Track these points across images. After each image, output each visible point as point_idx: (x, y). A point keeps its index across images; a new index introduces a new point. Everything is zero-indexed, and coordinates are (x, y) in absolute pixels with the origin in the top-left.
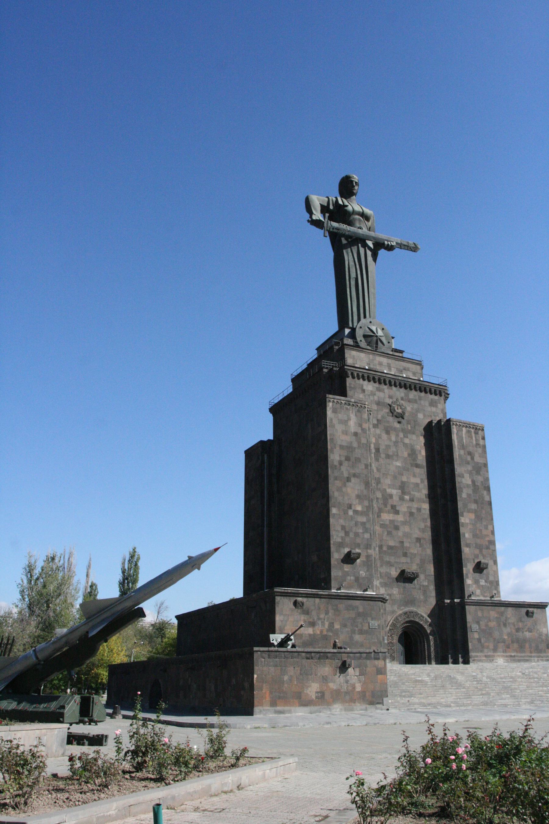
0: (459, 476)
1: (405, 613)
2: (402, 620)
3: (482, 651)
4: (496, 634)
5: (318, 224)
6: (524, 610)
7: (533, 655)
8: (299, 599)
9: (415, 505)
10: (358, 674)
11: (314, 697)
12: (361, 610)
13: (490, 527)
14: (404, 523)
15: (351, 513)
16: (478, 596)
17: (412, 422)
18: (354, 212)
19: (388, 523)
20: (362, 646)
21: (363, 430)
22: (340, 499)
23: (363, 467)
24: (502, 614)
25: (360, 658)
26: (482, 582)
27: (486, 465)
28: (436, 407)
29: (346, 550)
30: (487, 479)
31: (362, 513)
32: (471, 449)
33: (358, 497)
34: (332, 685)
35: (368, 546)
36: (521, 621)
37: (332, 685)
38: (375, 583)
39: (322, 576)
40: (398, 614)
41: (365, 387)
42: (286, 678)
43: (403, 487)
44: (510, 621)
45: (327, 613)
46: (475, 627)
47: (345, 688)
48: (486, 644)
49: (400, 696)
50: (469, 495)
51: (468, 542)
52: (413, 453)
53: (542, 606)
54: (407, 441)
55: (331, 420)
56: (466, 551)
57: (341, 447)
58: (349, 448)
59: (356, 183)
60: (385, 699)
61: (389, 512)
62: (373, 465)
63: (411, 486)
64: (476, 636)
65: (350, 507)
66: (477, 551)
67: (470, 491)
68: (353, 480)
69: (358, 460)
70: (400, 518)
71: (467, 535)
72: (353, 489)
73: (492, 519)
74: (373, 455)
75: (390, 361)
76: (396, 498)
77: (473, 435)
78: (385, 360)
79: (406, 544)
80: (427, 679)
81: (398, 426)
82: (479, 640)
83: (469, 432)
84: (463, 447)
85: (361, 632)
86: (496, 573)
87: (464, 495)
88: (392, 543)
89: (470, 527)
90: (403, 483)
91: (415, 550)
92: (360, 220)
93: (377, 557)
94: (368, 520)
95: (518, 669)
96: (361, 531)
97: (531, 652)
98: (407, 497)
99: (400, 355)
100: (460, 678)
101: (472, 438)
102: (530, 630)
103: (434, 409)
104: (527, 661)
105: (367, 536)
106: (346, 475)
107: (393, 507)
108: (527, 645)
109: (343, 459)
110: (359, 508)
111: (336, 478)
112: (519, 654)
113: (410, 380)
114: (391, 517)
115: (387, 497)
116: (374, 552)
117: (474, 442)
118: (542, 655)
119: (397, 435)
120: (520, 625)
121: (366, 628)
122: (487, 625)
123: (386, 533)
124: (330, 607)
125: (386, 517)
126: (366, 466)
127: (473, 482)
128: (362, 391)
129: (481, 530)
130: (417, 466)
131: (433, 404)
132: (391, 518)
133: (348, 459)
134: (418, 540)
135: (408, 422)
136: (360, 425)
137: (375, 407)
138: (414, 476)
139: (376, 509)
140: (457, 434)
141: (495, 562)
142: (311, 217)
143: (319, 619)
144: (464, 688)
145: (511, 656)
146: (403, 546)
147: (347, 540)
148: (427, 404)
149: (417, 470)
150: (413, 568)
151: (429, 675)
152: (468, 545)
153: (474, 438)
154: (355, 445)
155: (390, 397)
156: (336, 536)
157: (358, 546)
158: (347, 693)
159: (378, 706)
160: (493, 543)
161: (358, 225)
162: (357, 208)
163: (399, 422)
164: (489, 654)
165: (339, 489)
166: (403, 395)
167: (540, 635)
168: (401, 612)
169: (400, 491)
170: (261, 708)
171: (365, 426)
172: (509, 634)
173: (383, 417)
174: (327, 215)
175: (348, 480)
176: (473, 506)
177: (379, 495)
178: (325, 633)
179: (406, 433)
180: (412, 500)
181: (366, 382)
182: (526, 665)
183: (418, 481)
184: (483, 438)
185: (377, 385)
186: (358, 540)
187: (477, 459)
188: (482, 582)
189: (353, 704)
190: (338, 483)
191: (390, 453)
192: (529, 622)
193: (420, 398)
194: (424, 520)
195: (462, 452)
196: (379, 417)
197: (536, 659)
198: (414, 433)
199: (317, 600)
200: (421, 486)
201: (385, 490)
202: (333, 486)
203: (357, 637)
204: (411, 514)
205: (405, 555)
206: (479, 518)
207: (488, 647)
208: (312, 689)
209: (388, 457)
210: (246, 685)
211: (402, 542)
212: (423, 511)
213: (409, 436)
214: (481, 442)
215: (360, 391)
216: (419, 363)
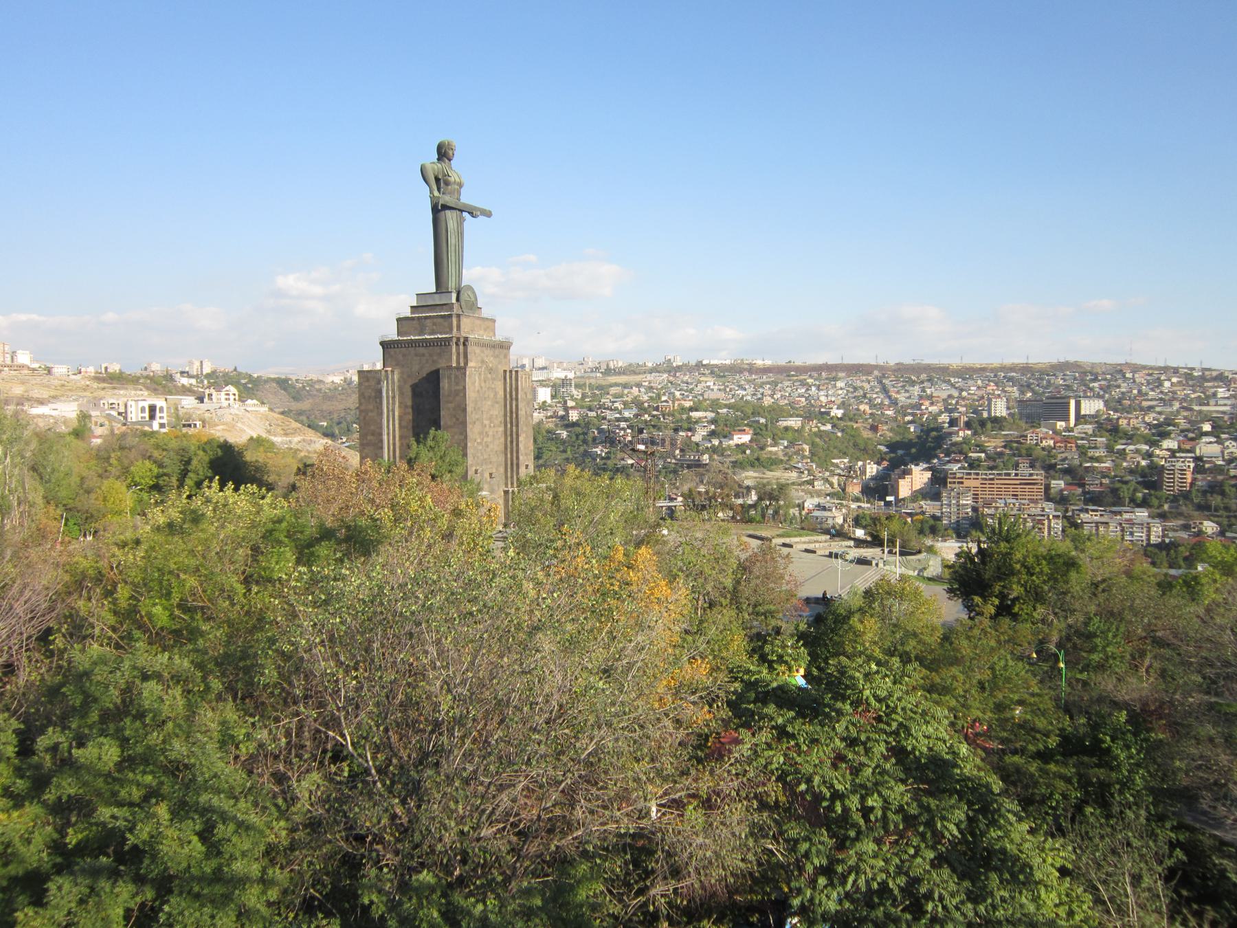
43: (490, 419)
52: (496, 394)
91: (494, 459)
179: (493, 379)
202: (469, 427)
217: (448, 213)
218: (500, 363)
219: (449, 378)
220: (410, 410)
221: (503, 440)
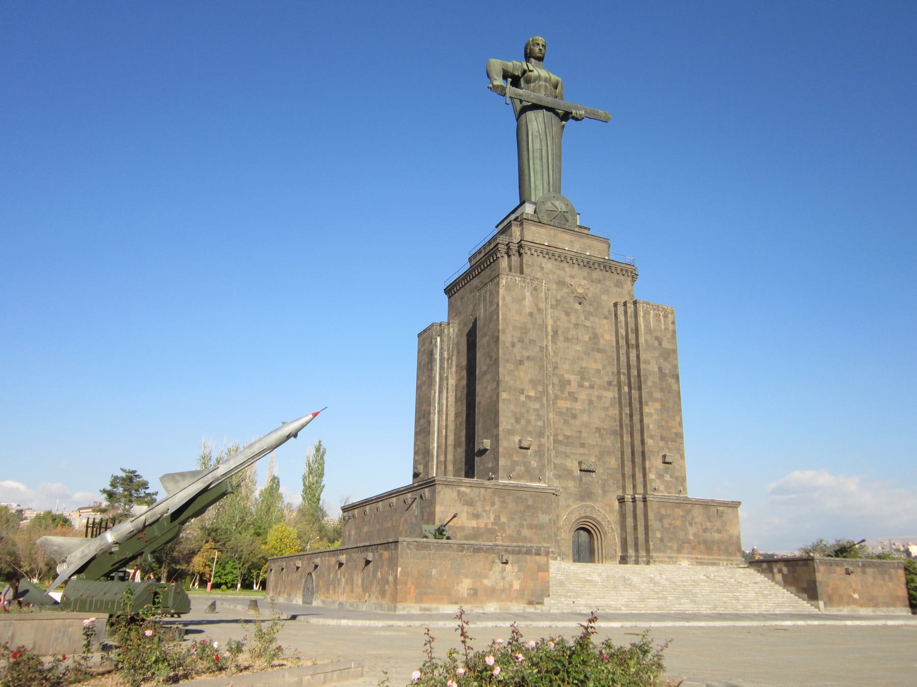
1: (582, 507)
2: (576, 516)
3: (664, 552)
4: (681, 534)
5: (501, 91)
7: (722, 557)
8: (463, 489)
9: (596, 392)
10: (516, 570)
11: (465, 595)
12: (530, 503)
13: (678, 419)
14: (583, 411)
15: (523, 398)
17: (595, 304)
18: (539, 78)
19: (564, 410)
20: (531, 541)
21: (539, 309)
22: (511, 383)
23: (538, 349)
24: (689, 511)
25: (519, 552)
26: (667, 477)
28: (622, 288)
30: (676, 367)
31: (537, 399)
32: (658, 334)
33: (531, 381)
34: (487, 582)
35: (541, 434)
36: (710, 521)
37: (487, 582)
38: (547, 474)
39: (490, 465)
40: (571, 509)
41: (543, 265)
43: (582, 374)
44: (697, 520)
45: (493, 504)
47: (501, 585)
48: (670, 544)
49: (566, 596)
50: (653, 382)
51: (653, 433)
52: (595, 338)
53: (735, 505)
55: (504, 299)
56: (649, 442)
57: (515, 328)
58: (524, 330)
60: (546, 600)
61: (566, 399)
62: (550, 348)
63: (592, 372)
64: (658, 535)
66: (662, 444)
67: (657, 380)
68: (526, 363)
69: (532, 342)
70: (578, 406)
71: (651, 426)
72: (528, 372)
73: (680, 410)
74: (550, 338)
75: (573, 238)
76: (574, 384)
77: (662, 318)
78: (567, 237)
79: (584, 434)
80: (596, 578)
82: (662, 540)
83: (657, 315)
84: (649, 331)
85: (531, 527)
86: (683, 468)
87: (650, 382)
88: (568, 433)
89: (655, 417)
90: (581, 368)
92: (546, 87)
93: (552, 447)
94: (542, 406)
95: (701, 573)
96: (533, 418)
97: (720, 555)
98: (586, 384)
99: (586, 231)
100: (635, 579)
101: (660, 321)
102: (719, 531)
103: (619, 290)
104: (713, 564)
105: (540, 423)
106: (518, 358)
107: (570, 394)
108: (715, 548)
109: (516, 340)
110: (532, 394)
111: (507, 361)
112: (706, 557)
114: (568, 404)
115: (564, 383)
116: (548, 442)
117: (663, 327)
118: (732, 558)
119: (578, 318)
120: (709, 525)
121: (535, 522)
122: (670, 524)
124: (496, 499)
125: (563, 404)
126: (541, 348)
127: (660, 369)
128: (542, 268)
129: (667, 422)
130: (599, 351)
131: (618, 284)
132: (568, 406)
133: (521, 340)
134: (598, 430)
135: (590, 304)
136: (537, 305)
137: (554, 287)
138: (596, 361)
139: (552, 396)
141: (682, 456)
142: (491, 83)
143: (484, 511)
144: (638, 590)
146: (580, 437)
147: (518, 427)
148: (612, 284)
149: (598, 356)
150: (591, 461)
151: (600, 575)
152: (651, 437)
154: (530, 326)
155: (572, 277)
156: (505, 422)
157: (530, 433)
158: (503, 590)
159: (538, 606)
160: (679, 435)
162: (544, 73)
163: (580, 304)
164: (673, 555)
165: (510, 372)
166: (585, 274)
167: (731, 537)
170: (404, 604)
171: (542, 305)
172: (695, 535)
173: (562, 297)
174: (510, 80)
175: (521, 362)
176: (657, 395)
177: (556, 381)
178: (490, 526)
179: (588, 315)
180: (592, 387)
181: (544, 260)
182: (712, 568)
183: (601, 368)
184: (673, 323)
185: (558, 263)
186: (530, 428)
187: (665, 344)
188: (667, 477)
189: (510, 604)
190: (510, 366)
191: (570, 336)
192: (718, 524)
193: (605, 279)
194: (606, 409)
195: (649, 337)
196: (559, 297)
197: (725, 563)
198: (596, 316)
199: (483, 490)
200: (603, 372)
202: (504, 369)
203: (526, 532)
204: (591, 402)
205: (583, 445)
206: (664, 408)
207: (671, 548)
208: (465, 585)
210: (391, 579)
211: (580, 432)
212: (604, 400)
213: (592, 318)
214: (671, 327)
215: (538, 269)
216: (606, 241)
217: (530, 115)
218: (606, 291)
219: (485, 299)
220: (464, 373)
221: (614, 412)
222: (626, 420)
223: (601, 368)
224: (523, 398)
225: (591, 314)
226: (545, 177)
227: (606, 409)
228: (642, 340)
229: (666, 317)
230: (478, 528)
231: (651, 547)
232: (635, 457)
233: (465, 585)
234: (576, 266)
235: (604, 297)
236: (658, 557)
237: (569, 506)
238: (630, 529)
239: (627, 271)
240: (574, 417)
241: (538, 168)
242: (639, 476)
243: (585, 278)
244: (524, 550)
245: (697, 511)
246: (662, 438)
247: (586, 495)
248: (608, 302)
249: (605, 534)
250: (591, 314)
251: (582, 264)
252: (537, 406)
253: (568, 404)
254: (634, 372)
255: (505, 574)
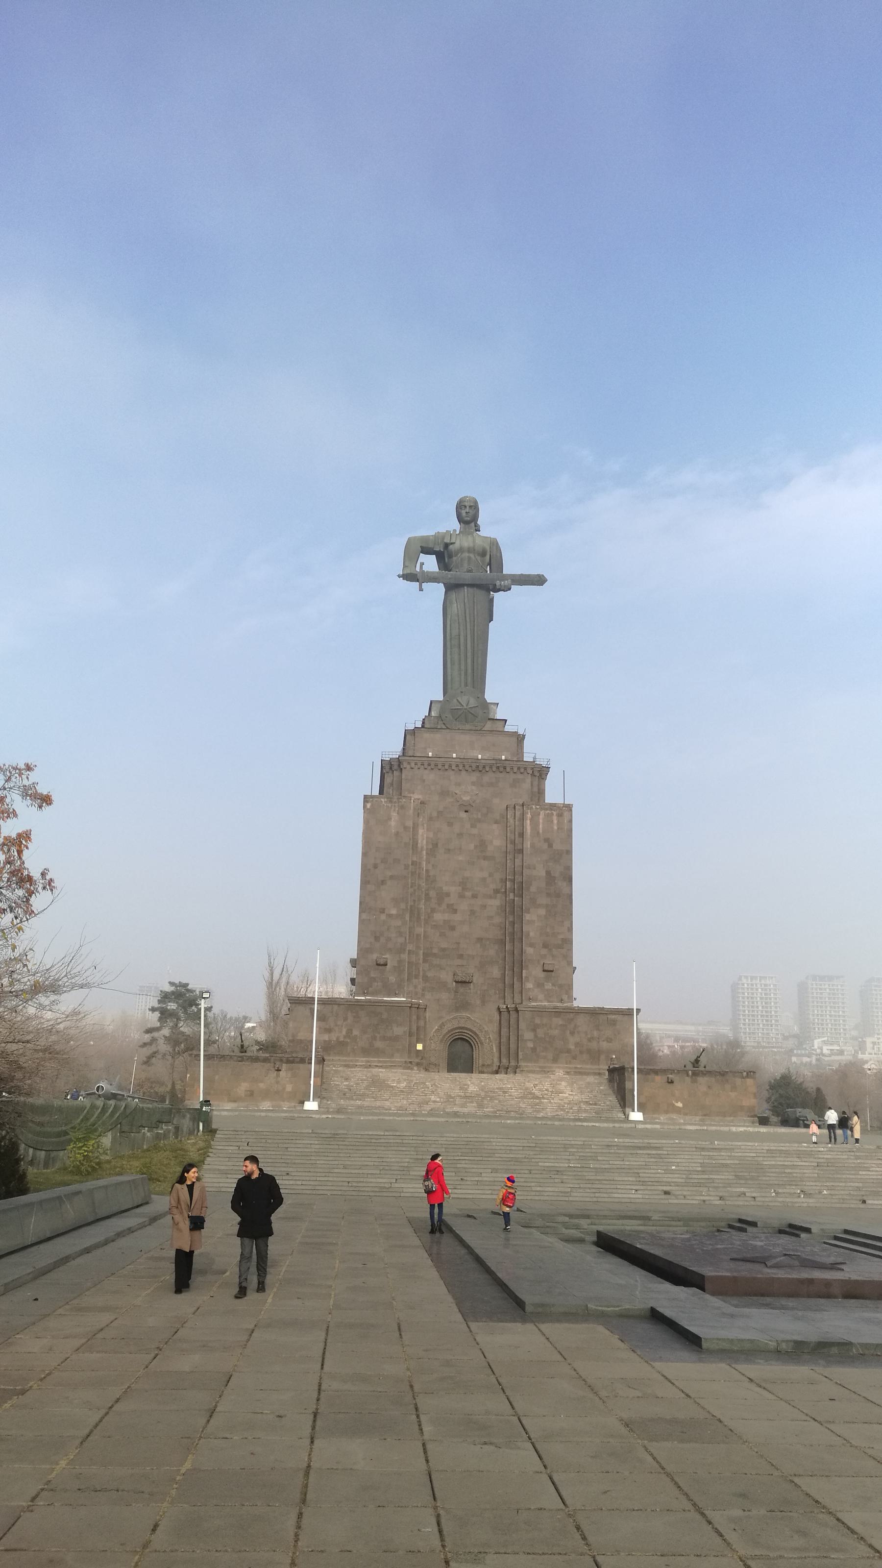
0: (529, 868)
2: (449, 1026)
6: (605, 1017)
10: (289, 1075)
12: (385, 1016)
13: (567, 924)
16: (541, 1001)
18: (461, 550)
21: (406, 828)
25: (293, 1062)
27: (569, 852)
29: (375, 956)
30: (569, 868)
34: (262, 1085)
35: (401, 950)
36: (598, 1029)
42: (217, 1077)
46: (528, 1035)
48: (544, 1054)
52: (482, 844)
54: (475, 831)
56: (529, 951)
59: (470, 507)
64: (530, 1045)
65: (382, 911)
66: (544, 951)
71: (532, 934)
73: (572, 915)
81: (463, 815)
82: (534, 1050)
85: (384, 1038)
88: (444, 945)
92: (469, 558)
98: (468, 894)
101: (552, 822)
102: (609, 1040)
105: (401, 940)
107: (448, 906)
108: (603, 1057)
110: (394, 912)
112: (589, 1066)
113: (483, 761)
114: (446, 916)
115: (442, 896)
117: (556, 828)
120: (596, 1033)
123: (438, 934)
125: (438, 917)
126: (406, 867)
127: (548, 873)
130: (485, 858)
133: (384, 861)
134: (480, 940)
140: (531, 820)
145: (576, 1068)
149: (485, 864)
152: (532, 945)
153: (555, 822)
155: (458, 784)
161: (466, 565)
168: (448, 1018)
169: (460, 888)
175: (383, 882)
176: (543, 900)
178: (342, 1039)
181: (426, 772)
183: (485, 874)
184: (571, 821)
187: (557, 846)
196: (441, 809)
199: (336, 1007)
201: (441, 888)
204: (472, 912)
205: (461, 956)
208: (243, 1087)
209: (448, 851)
211: (458, 943)
222: (509, 929)
223: (485, 874)
224: (383, 917)
225: (479, 821)
226: (463, 667)
227: (490, 918)
228: (528, 844)
229: (560, 815)
230: (330, 1041)
231: (520, 1057)
232: (516, 966)
233: (243, 1087)
234: (464, 773)
235: (496, 801)
236: (527, 1066)
237: (440, 1018)
238: (504, 1040)
239: (525, 769)
240: (453, 928)
241: (456, 657)
242: (517, 985)
243: (473, 784)
244: (298, 1060)
245: (582, 1021)
246: (545, 946)
247: (463, 1005)
248: (499, 805)
249: (482, 1044)
250: (479, 821)
251: (470, 769)
252: (399, 923)
253: (446, 916)
254: (518, 878)
255: (279, 1079)
